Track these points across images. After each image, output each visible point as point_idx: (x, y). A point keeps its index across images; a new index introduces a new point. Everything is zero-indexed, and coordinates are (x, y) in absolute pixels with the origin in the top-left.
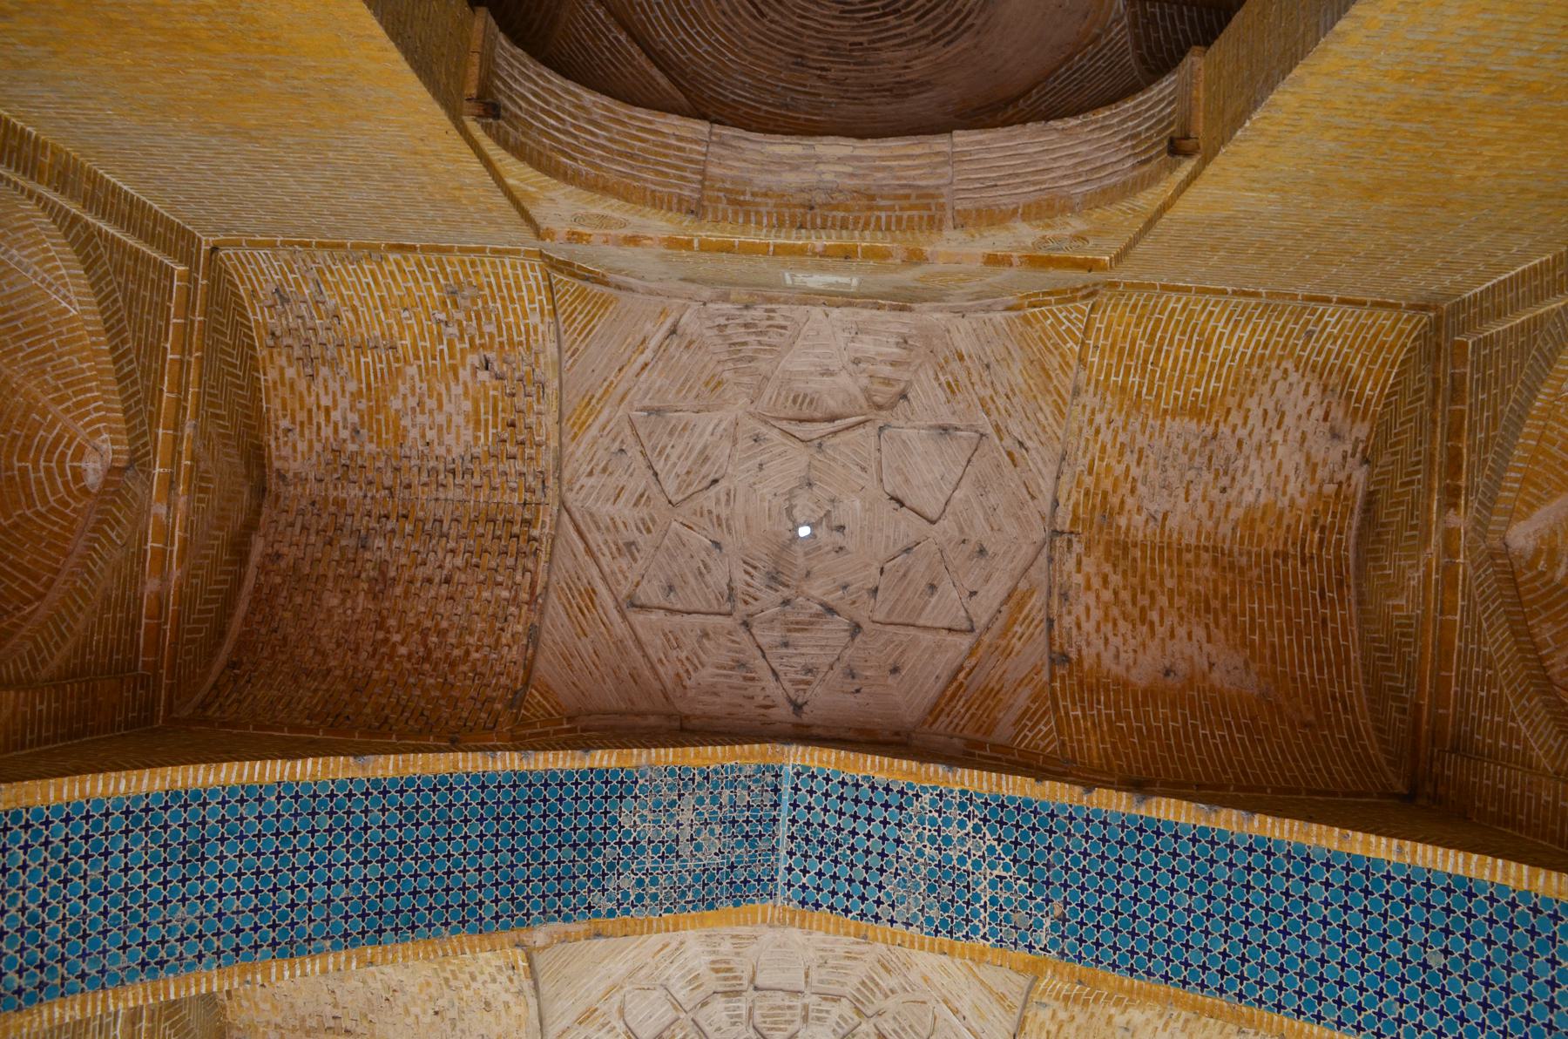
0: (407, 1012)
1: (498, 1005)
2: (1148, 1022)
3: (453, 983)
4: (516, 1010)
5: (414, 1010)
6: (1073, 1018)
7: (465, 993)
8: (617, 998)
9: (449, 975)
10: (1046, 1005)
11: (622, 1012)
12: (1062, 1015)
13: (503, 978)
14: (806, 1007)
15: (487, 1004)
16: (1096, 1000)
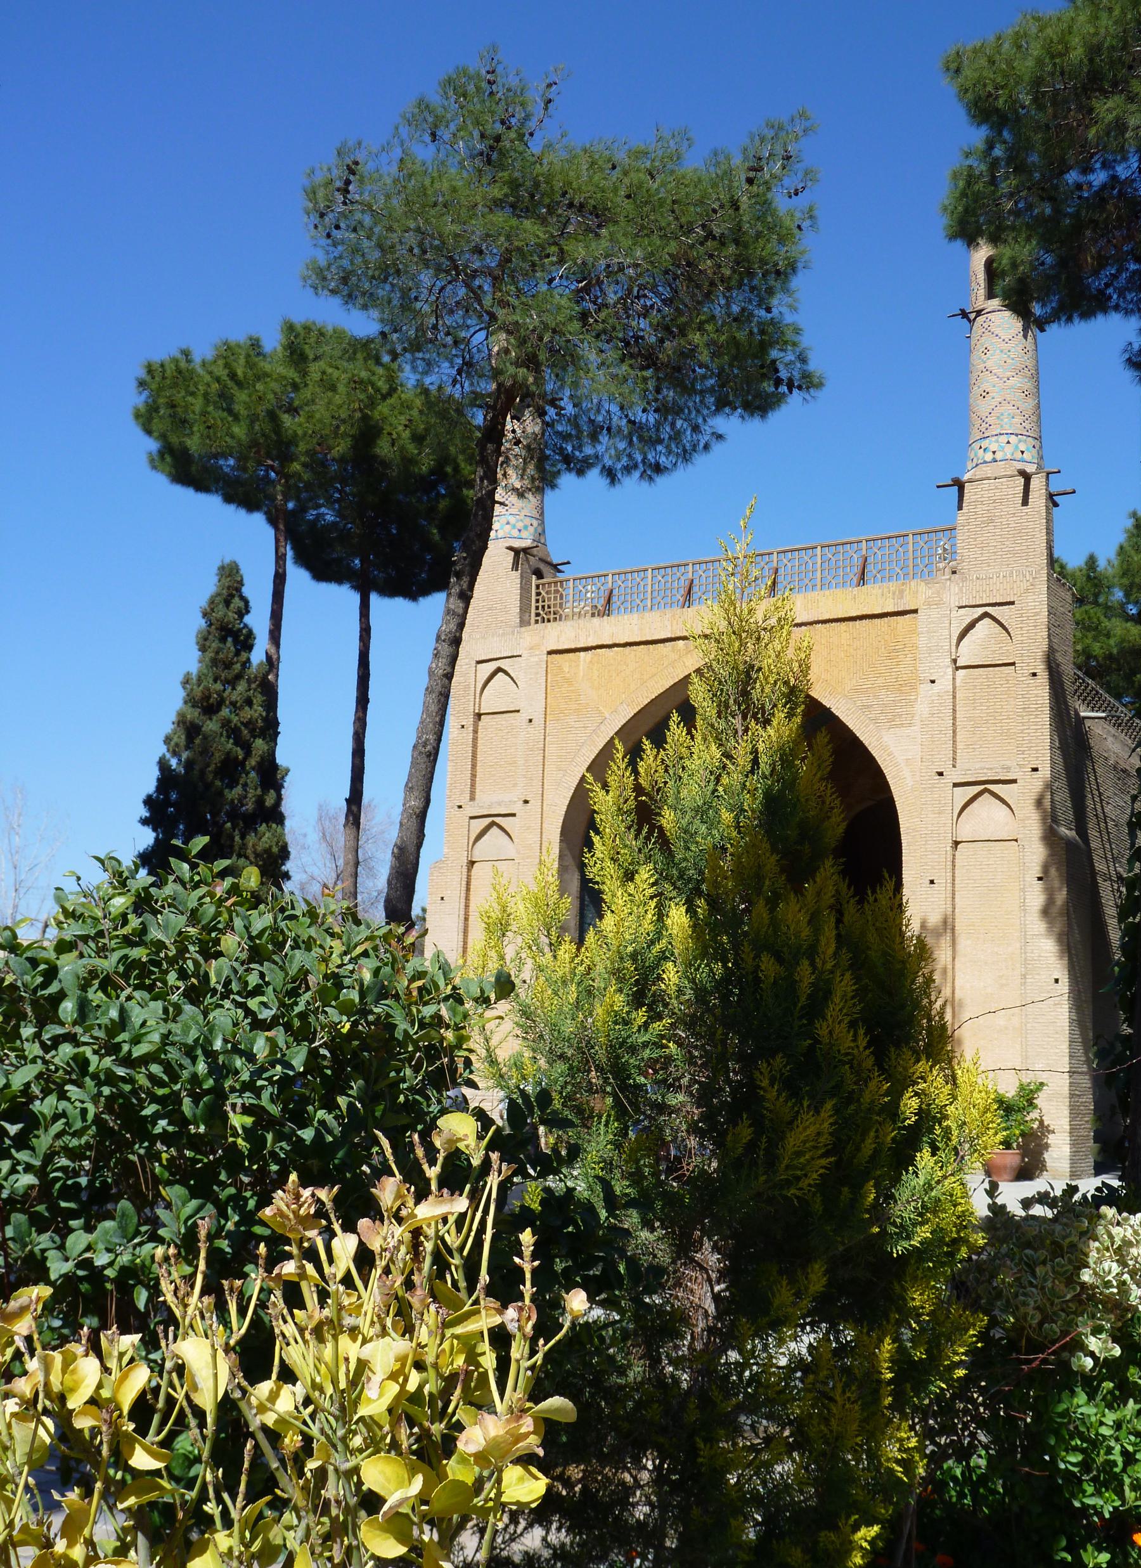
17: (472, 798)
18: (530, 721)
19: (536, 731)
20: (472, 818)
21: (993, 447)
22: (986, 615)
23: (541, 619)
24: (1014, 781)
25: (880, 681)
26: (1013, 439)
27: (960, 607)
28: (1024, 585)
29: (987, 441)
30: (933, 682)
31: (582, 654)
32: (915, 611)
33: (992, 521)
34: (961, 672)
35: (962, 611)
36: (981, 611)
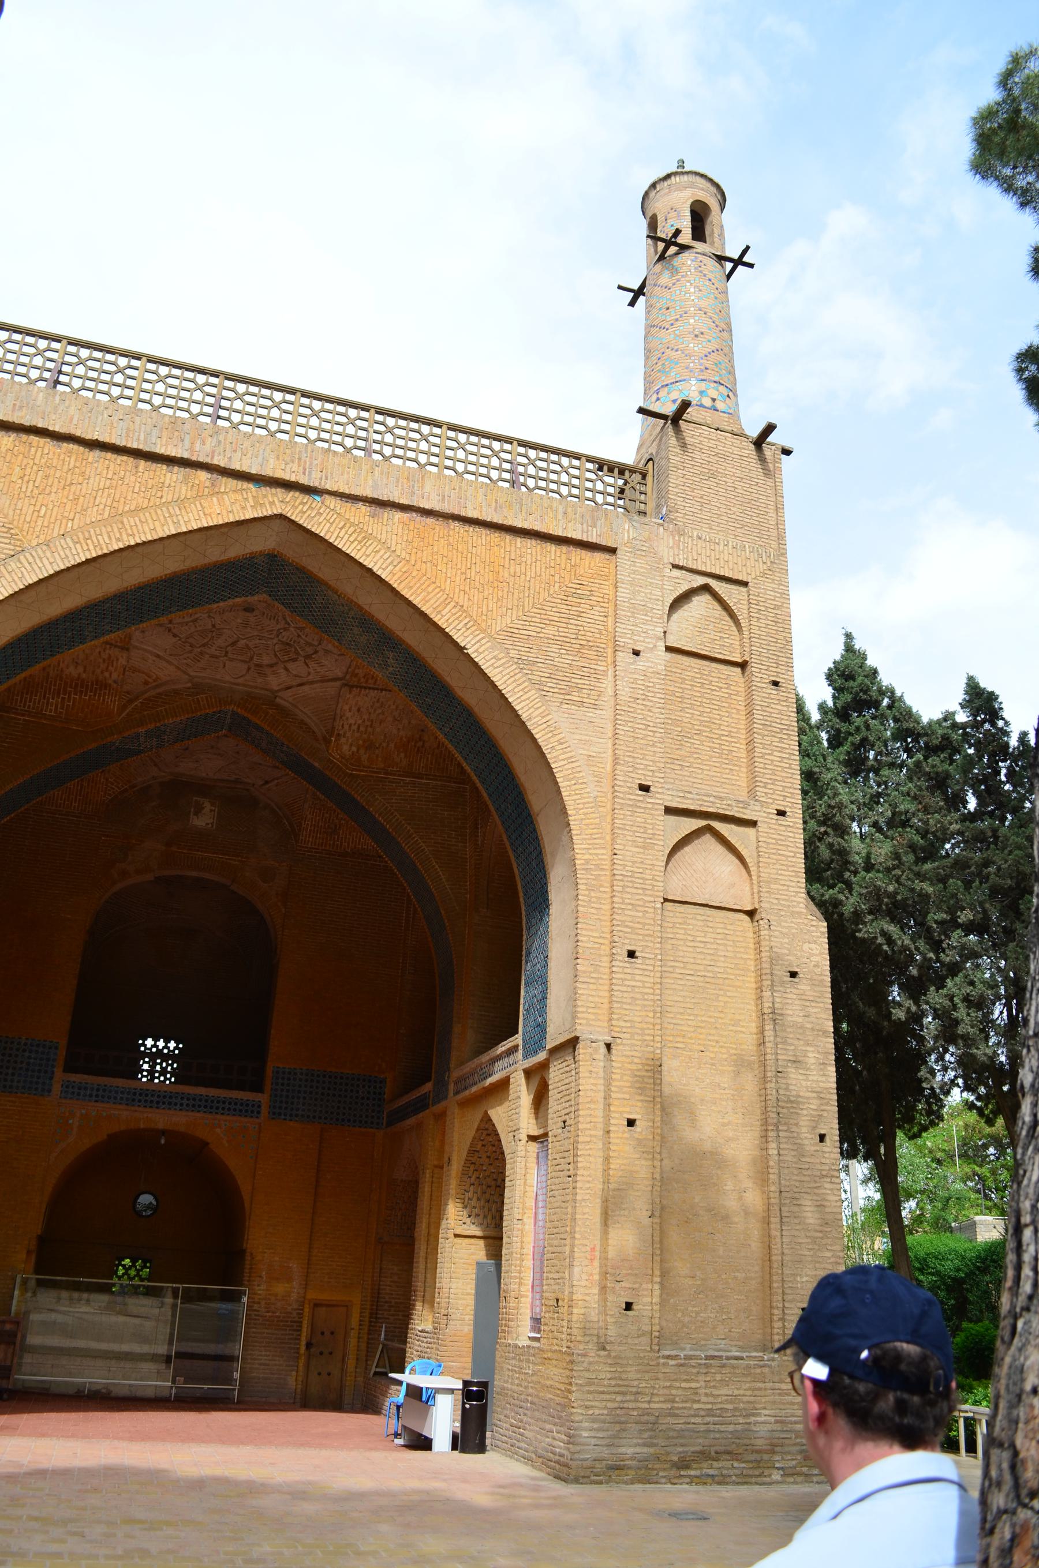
0: (397, 707)
1: (354, 709)
2: (68, 667)
3: (369, 723)
4: (347, 707)
5: (394, 707)
6: (102, 672)
7: (366, 717)
8: (311, 677)
9: (370, 729)
10: (115, 682)
11: (309, 674)
12: (107, 674)
13: (346, 727)
14: (226, 655)
15: (359, 710)
16: (92, 684)
22: (706, 588)
24: (753, 824)
25: (550, 631)
27: (676, 567)
30: (636, 653)
32: (613, 551)
36: (701, 580)
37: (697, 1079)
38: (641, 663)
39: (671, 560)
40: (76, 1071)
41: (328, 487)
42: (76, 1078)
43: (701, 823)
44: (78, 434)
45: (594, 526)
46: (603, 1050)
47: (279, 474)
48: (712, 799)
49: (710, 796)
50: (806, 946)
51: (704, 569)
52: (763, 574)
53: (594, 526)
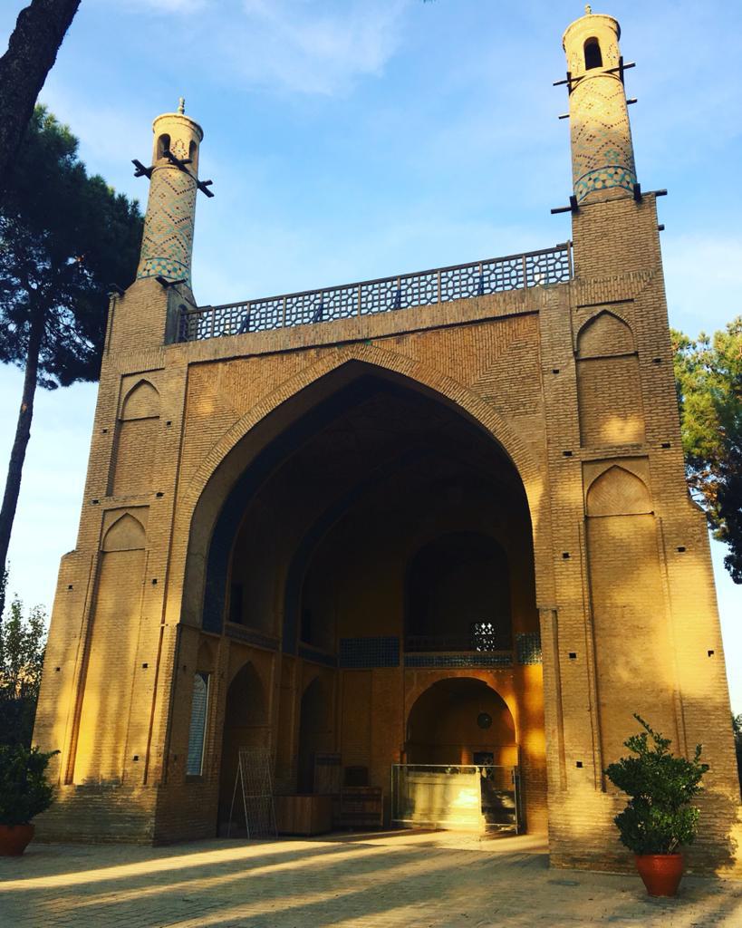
17: (110, 493)
18: (169, 423)
19: (174, 433)
20: (106, 511)
21: (603, 177)
23: (183, 339)
25: (503, 375)
26: (619, 171)
28: (643, 285)
29: (596, 173)
30: (556, 372)
31: (220, 365)
32: (537, 312)
33: (606, 235)
34: (583, 365)
35: (582, 311)
36: (599, 309)
37: (622, 624)
38: (560, 377)
39: (576, 304)
40: (412, 650)
41: (372, 336)
42: (410, 655)
43: (610, 465)
44: (254, 353)
45: (523, 301)
46: (551, 615)
47: (348, 338)
48: (614, 449)
49: (612, 448)
50: (690, 530)
51: (600, 301)
52: (644, 290)
53: (523, 301)
